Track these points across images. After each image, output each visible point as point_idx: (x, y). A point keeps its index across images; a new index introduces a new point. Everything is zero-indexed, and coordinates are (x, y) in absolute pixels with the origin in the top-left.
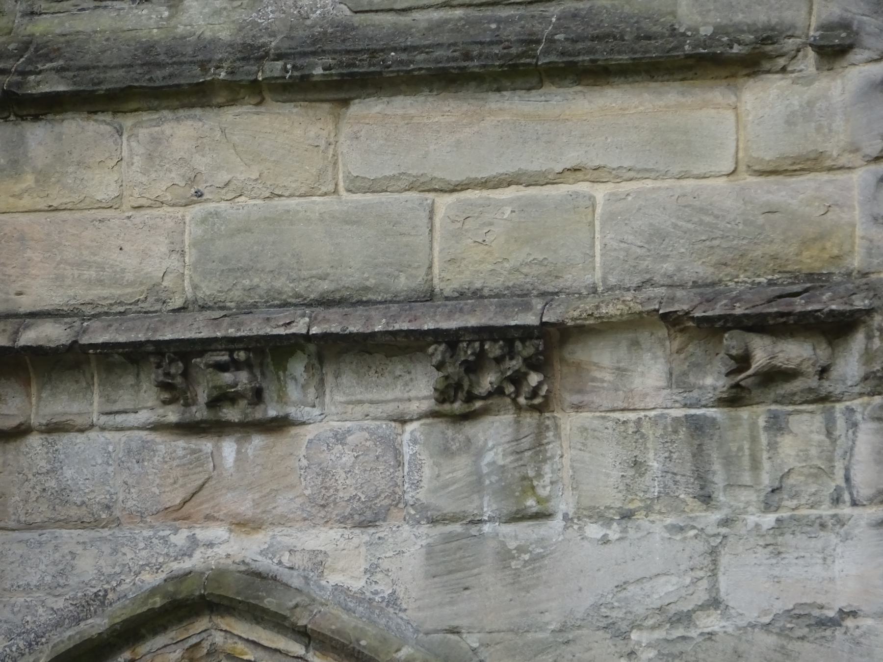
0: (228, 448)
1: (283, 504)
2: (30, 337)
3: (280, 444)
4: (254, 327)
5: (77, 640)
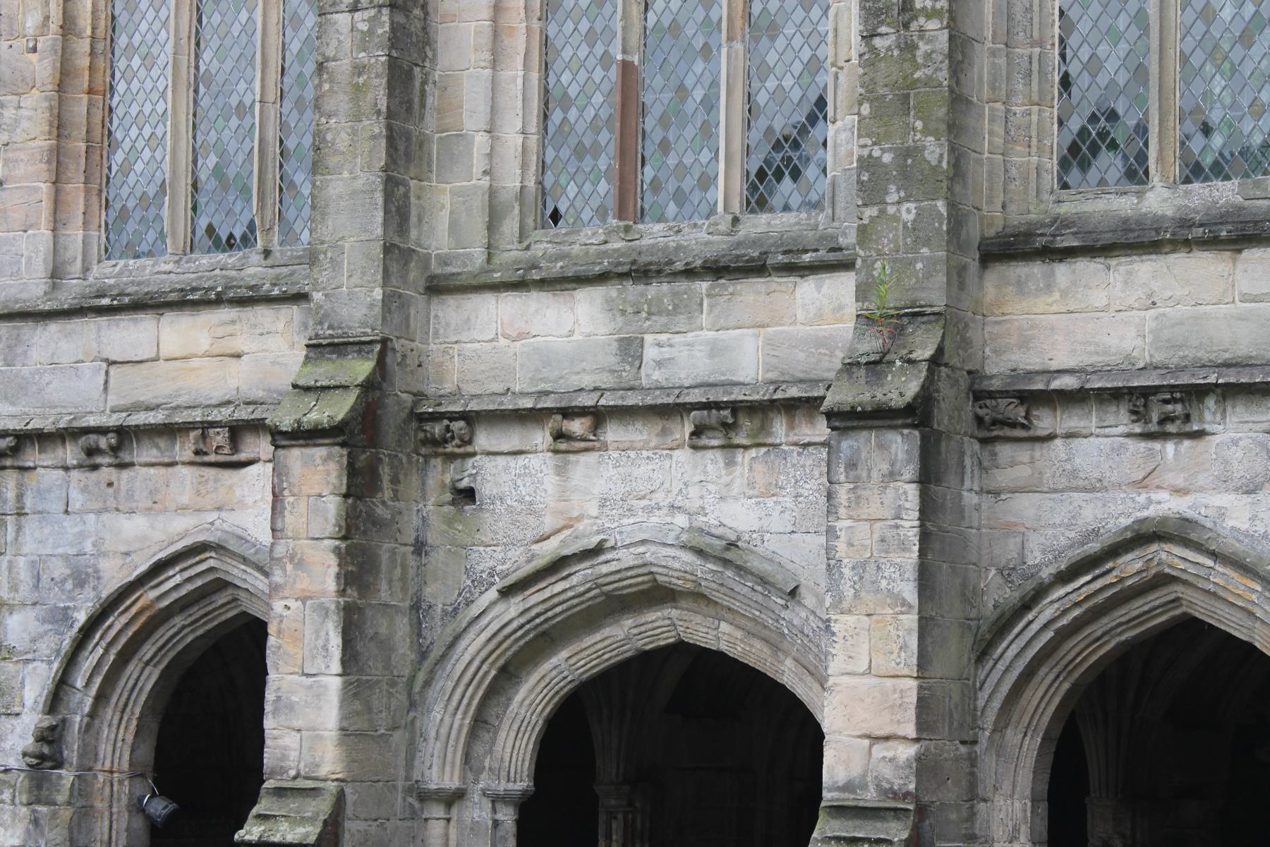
0: (1170, 447)
1: (1202, 480)
2: (1056, 384)
3: (1200, 445)
4: (1185, 379)
5: (1082, 556)
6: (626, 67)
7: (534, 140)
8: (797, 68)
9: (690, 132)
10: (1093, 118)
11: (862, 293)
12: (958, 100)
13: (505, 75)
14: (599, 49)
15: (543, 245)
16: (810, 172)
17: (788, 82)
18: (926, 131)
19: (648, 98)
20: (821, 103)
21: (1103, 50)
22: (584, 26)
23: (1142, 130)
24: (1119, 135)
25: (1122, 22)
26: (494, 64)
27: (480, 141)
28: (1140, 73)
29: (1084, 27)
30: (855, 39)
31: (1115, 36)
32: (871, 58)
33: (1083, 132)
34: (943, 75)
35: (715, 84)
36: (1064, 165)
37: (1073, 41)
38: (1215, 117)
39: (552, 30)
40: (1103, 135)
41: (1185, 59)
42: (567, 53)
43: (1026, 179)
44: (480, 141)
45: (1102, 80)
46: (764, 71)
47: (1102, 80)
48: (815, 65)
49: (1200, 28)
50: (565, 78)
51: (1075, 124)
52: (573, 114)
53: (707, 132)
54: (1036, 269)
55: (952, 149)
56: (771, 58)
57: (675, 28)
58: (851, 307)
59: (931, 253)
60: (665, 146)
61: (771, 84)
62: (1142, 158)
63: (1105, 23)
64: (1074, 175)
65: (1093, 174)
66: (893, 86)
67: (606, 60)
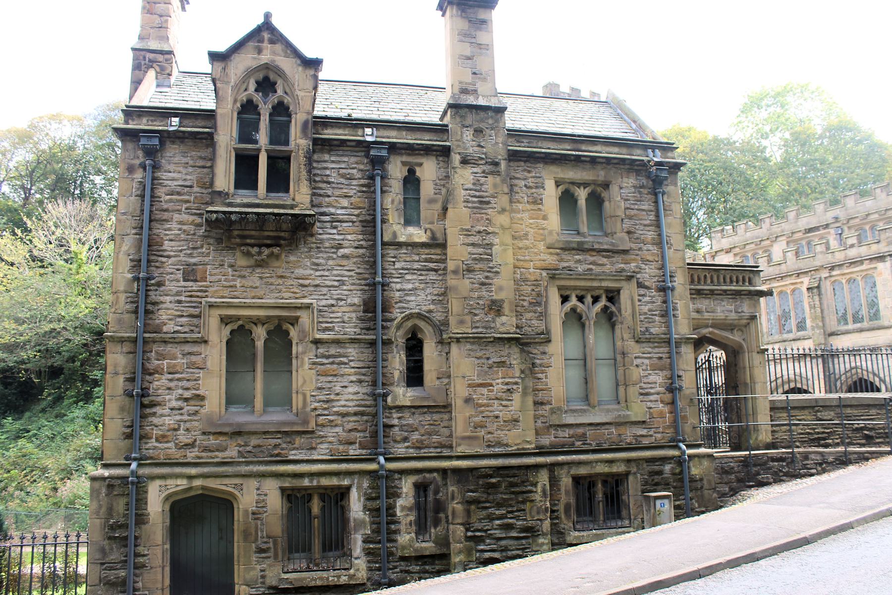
11: (814, 342)
12: (823, 317)
15: (770, 338)
32: (811, 313)
54: (835, 337)
58: (812, 343)
59: (822, 337)
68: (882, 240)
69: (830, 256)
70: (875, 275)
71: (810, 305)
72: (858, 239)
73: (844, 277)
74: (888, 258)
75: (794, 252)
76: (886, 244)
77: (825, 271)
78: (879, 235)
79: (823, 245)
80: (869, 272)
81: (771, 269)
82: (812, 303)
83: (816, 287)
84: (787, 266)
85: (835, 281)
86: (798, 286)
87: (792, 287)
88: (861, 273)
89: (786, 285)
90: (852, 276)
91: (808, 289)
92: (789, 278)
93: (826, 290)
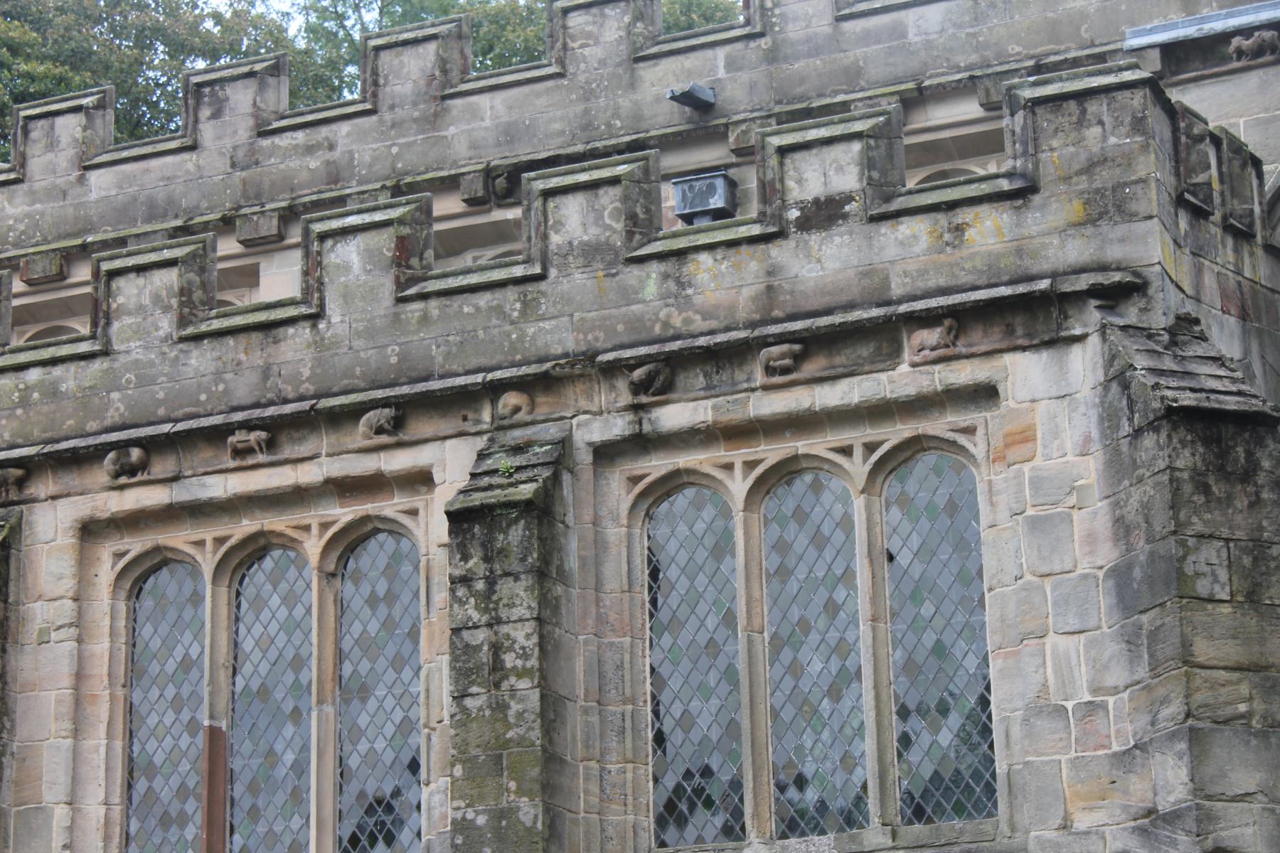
6: (214, 733)
7: (117, 811)
8: (389, 729)
9: (280, 797)
10: (688, 775)
12: (552, 760)
13: (88, 744)
14: (186, 716)
16: (405, 836)
17: (380, 745)
18: (520, 792)
19: (236, 764)
20: (414, 766)
21: (695, 705)
22: (170, 692)
23: (736, 785)
24: (714, 791)
25: (712, 679)
26: (77, 732)
27: (61, 814)
28: (732, 729)
29: (675, 683)
30: (447, 700)
31: (705, 692)
32: (463, 718)
33: (678, 789)
34: (536, 735)
35: (305, 748)
36: (661, 822)
37: (665, 698)
38: (808, 769)
39: (137, 697)
40: (699, 791)
41: (775, 714)
42: (152, 720)
43: (623, 839)
44: (61, 814)
45: (695, 736)
46: (355, 733)
47: (695, 736)
48: (407, 727)
49: (788, 682)
50: (151, 745)
51: (670, 781)
52: (158, 782)
53: (298, 797)
55: (547, 810)
56: (363, 720)
57: (264, 692)
60: (254, 813)
61: (363, 746)
62: (738, 813)
63: (696, 678)
64: (671, 833)
65: (691, 832)
66: (486, 747)
67: (193, 727)
68: (1048, 173)
69: (650, 281)
70: (977, 448)
71: (461, 653)
72: (868, 163)
73: (739, 455)
74: (1092, 315)
75: (384, 241)
76: (1075, 210)
77: (602, 398)
78: (1032, 143)
79: (609, 199)
80: (938, 425)
81: (200, 360)
82: (480, 637)
83: (526, 507)
84: (319, 344)
85: (671, 484)
86: (390, 506)
87: (343, 513)
88: (870, 433)
89: (298, 496)
90: (802, 445)
91: (459, 519)
92: (323, 442)
93: (600, 544)
